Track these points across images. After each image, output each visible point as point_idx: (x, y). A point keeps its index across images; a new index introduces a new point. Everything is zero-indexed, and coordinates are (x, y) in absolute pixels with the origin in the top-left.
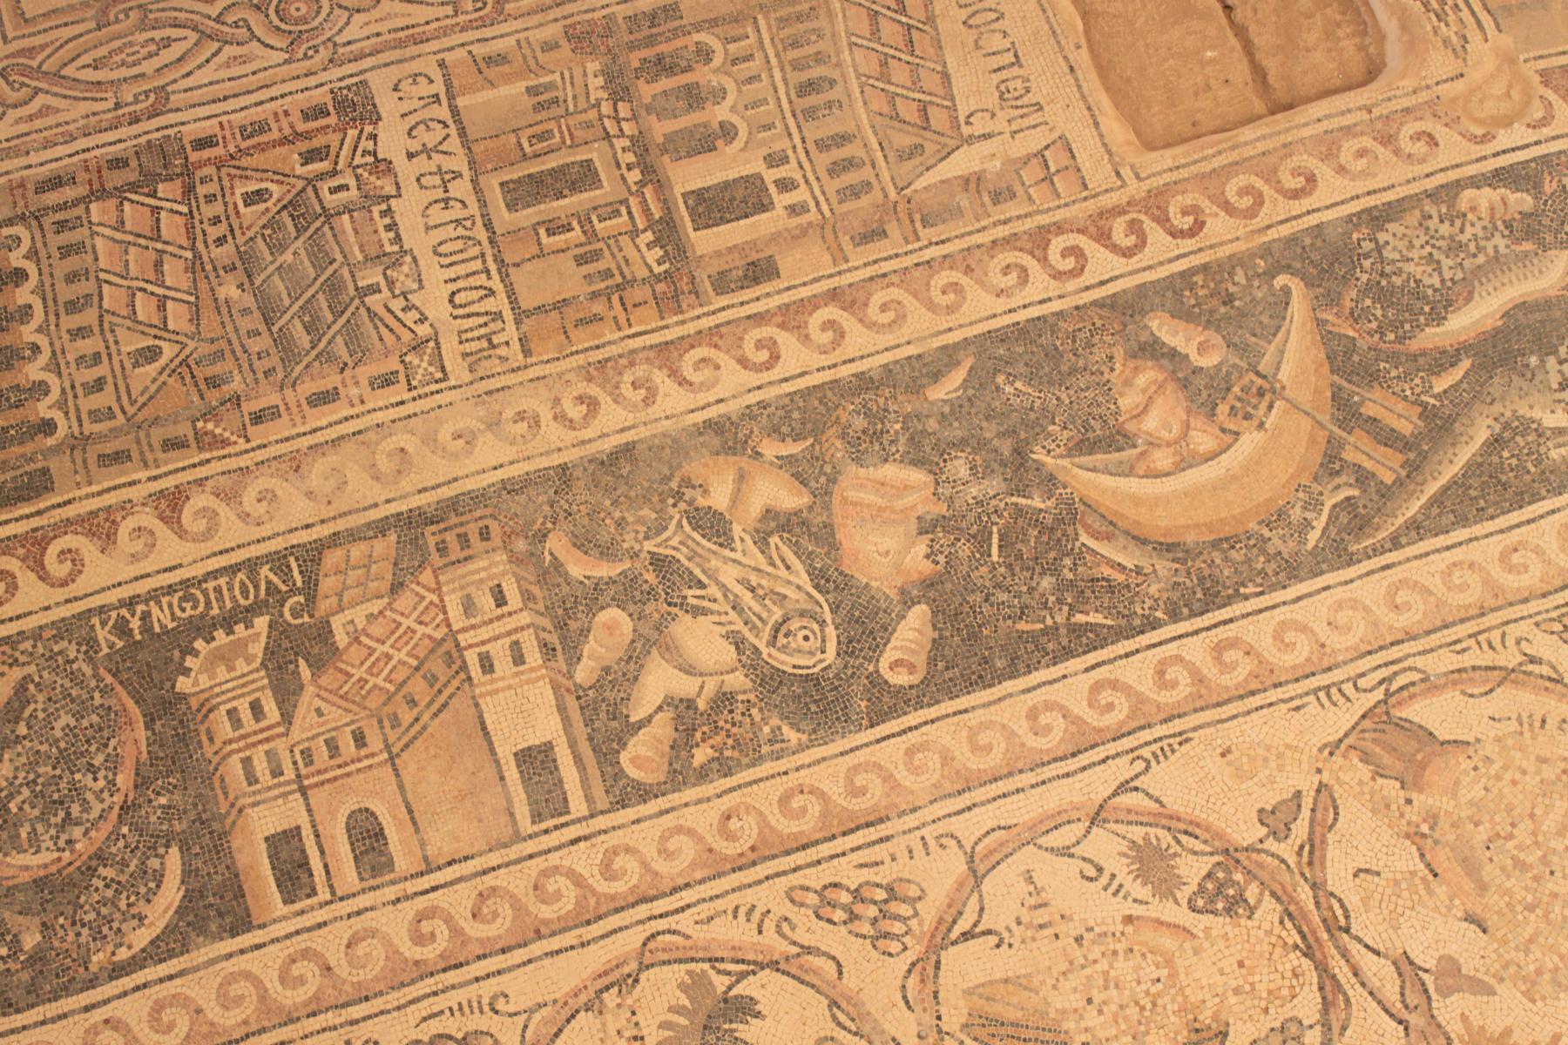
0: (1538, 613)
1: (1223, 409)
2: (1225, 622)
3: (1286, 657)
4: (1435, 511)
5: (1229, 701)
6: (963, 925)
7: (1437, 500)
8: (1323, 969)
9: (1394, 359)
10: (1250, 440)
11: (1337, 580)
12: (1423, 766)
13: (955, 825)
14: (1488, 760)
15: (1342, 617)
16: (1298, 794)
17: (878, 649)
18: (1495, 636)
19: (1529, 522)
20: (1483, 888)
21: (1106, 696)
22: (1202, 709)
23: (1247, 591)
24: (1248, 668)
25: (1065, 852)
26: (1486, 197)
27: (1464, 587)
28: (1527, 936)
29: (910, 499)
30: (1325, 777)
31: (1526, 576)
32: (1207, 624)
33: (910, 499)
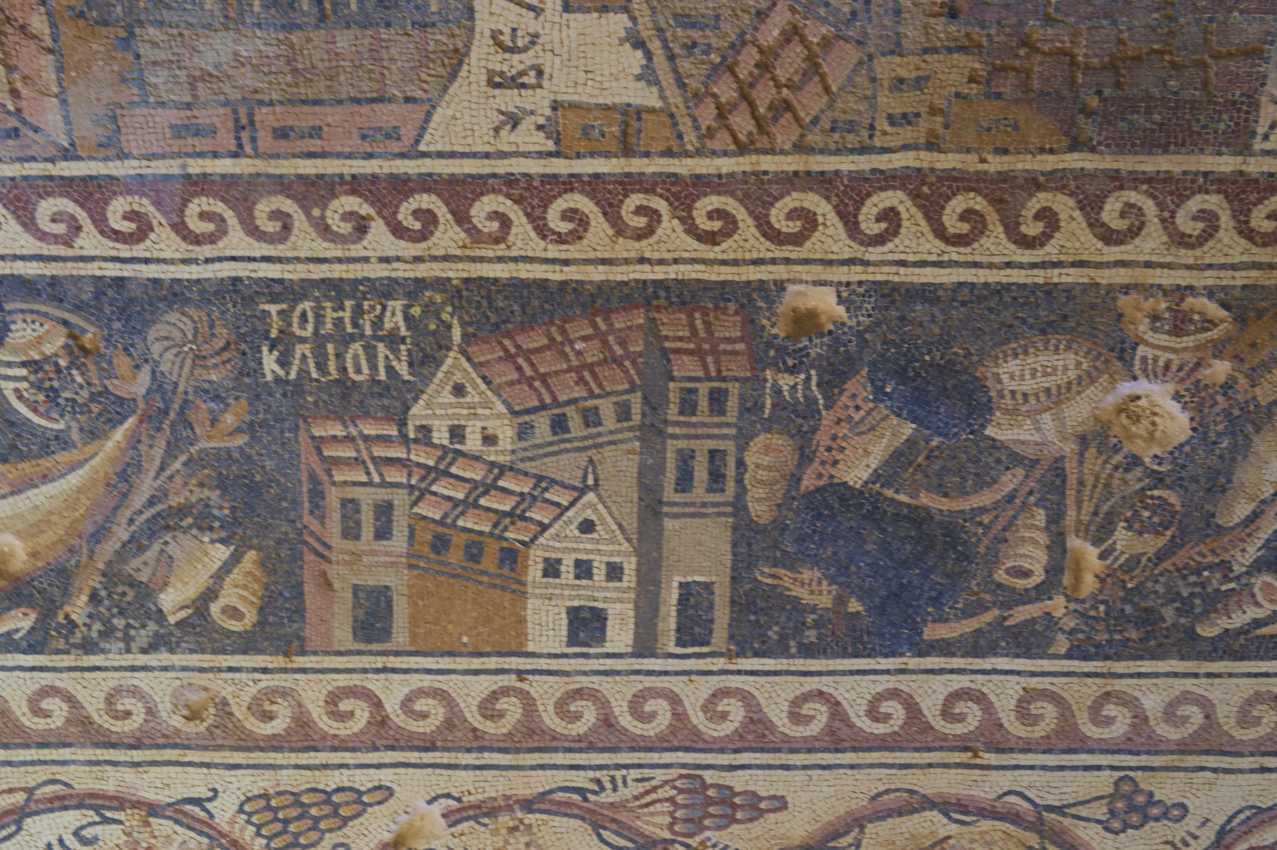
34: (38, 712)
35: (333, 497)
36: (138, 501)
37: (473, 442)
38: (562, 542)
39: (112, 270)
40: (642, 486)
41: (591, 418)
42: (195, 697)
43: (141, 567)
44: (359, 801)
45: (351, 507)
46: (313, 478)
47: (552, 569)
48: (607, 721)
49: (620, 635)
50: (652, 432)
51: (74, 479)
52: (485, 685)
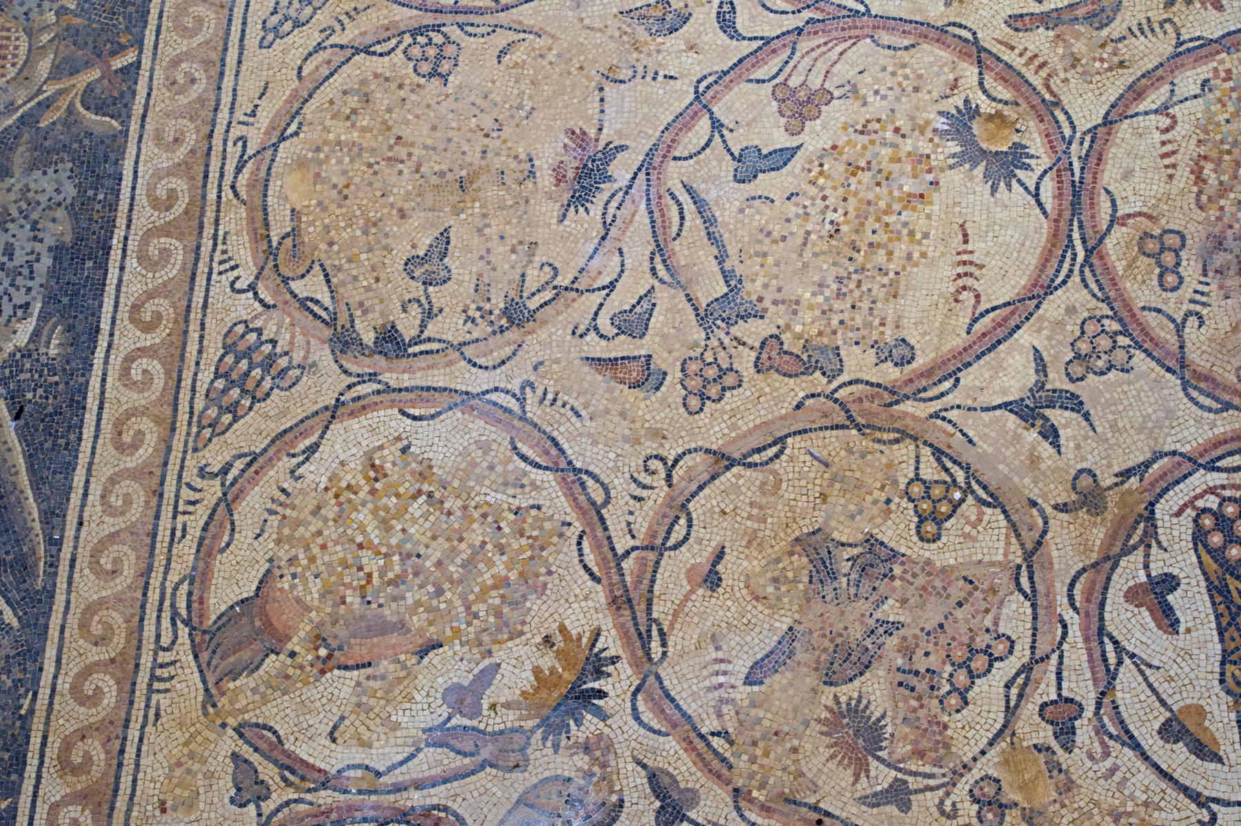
0: (186, 442)
2: (44, 744)
3: (106, 702)
4: (46, 490)
5: (117, 778)
7: (36, 484)
11: (60, 616)
12: (268, 623)
14: (292, 561)
15: (96, 629)
16: (235, 756)
18: (186, 494)
19: (101, 408)
20: (401, 627)
22: (112, 809)
23: (26, 707)
24: (97, 743)
27: (128, 500)
28: (462, 609)
30: (231, 721)
31: (148, 436)
32: (36, 762)
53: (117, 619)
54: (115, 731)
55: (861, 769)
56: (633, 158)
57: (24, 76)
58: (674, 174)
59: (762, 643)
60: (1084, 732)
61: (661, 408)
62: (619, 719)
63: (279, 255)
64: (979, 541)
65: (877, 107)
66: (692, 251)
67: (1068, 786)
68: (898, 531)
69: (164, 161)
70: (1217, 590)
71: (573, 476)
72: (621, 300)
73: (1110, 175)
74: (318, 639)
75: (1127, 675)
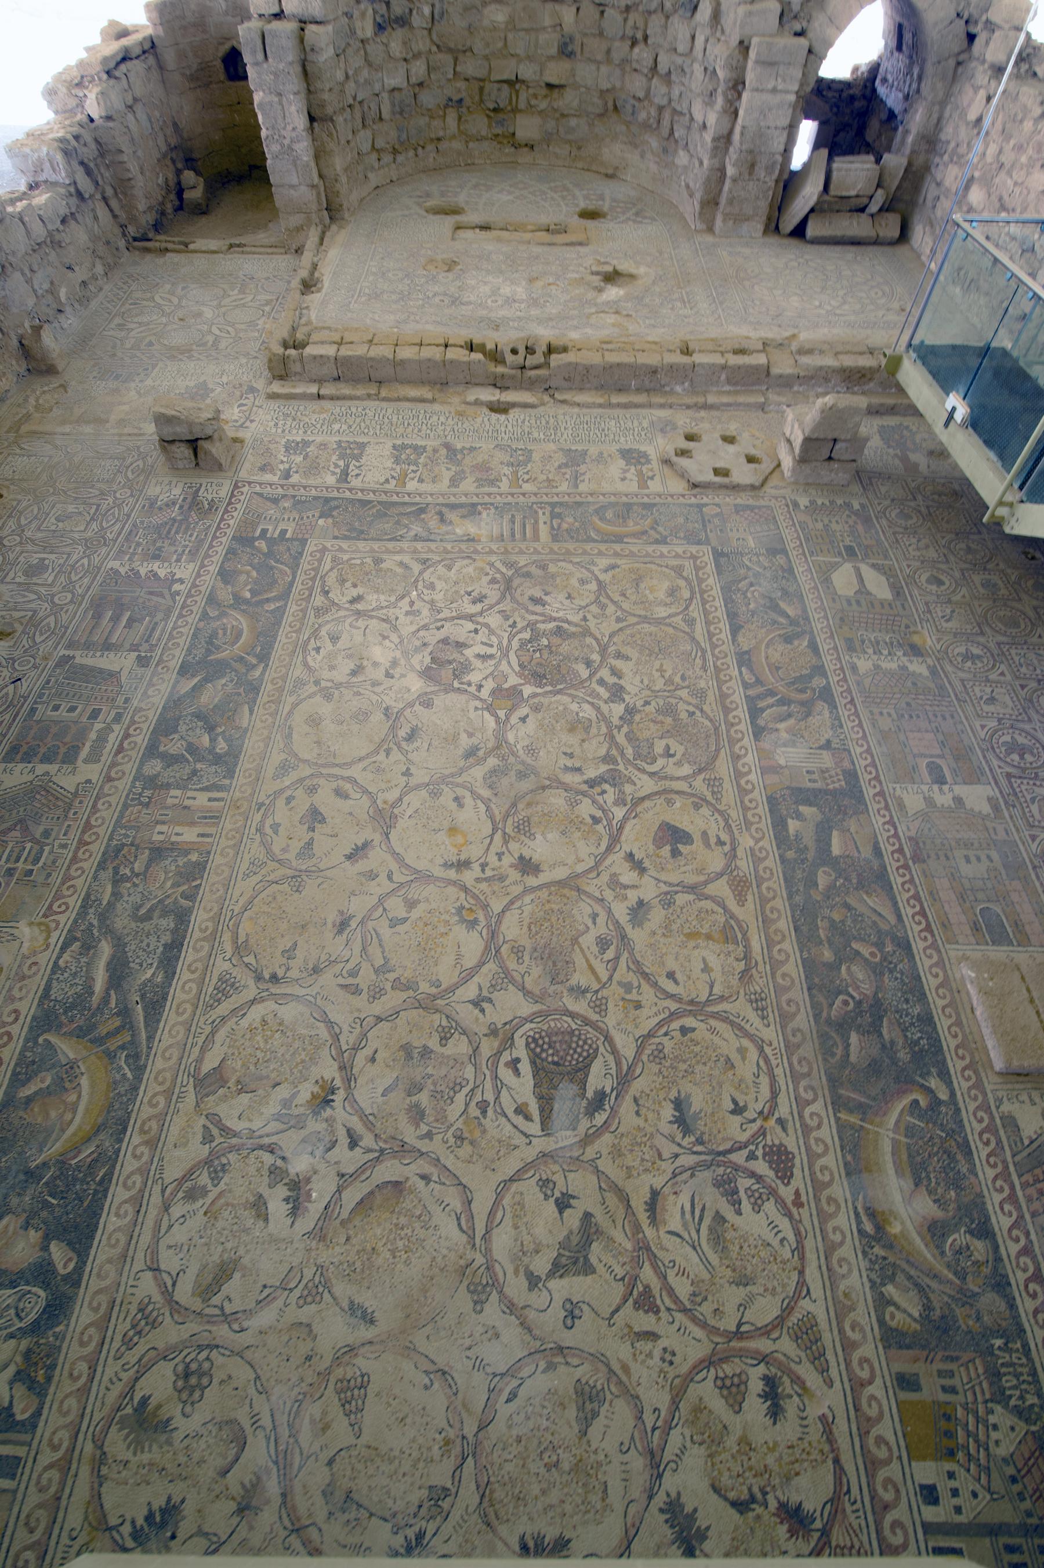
1: (67, 1085)
6: (169, 1283)
7: (147, 1026)
8: (261, 1147)
9: (93, 1015)
10: (84, 1081)
13: (135, 1270)
17: (54, 1272)
21: (130, 1182)
25: (171, 1226)
26: (66, 956)
29: (11, 1229)
33: (11, 1229)
34: (835, 1229)
35: (953, 1366)
36: (927, 1280)
37: (994, 1435)
38: (965, 1482)
39: (1013, 1282)
40: (1001, 1525)
41: (1021, 1496)
42: (854, 1296)
43: (900, 1278)
44: (824, 1370)
45: (951, 1374)
46: (957, 1358)
47: (951, 1475)
48: (886, 1507)
49: (930, 1513)
50: (1026, 1530)
51: (929, 1256)
52: (891, 1438)
53: (168, 1075)
54: (162, 1118)
55: (417, 1126)
56: (358, 919)
57: (161, 887)
58: (370, 925)
59: (388, 1081)
60: (490, 1112)
61: (360, 1001)
62: (339, 1112)
63: (240, 949)
64: (459, 1046)
65: (434, 905)
66: (374, 950)
67: (484, 1131)
68: (433, 1043)
69: (206, 916)
70: (533, 1063)
71: (330, 1024)
72: (350, 966)
73: (503, 928)
74: (238, 1082)
75: (504, 1092)
